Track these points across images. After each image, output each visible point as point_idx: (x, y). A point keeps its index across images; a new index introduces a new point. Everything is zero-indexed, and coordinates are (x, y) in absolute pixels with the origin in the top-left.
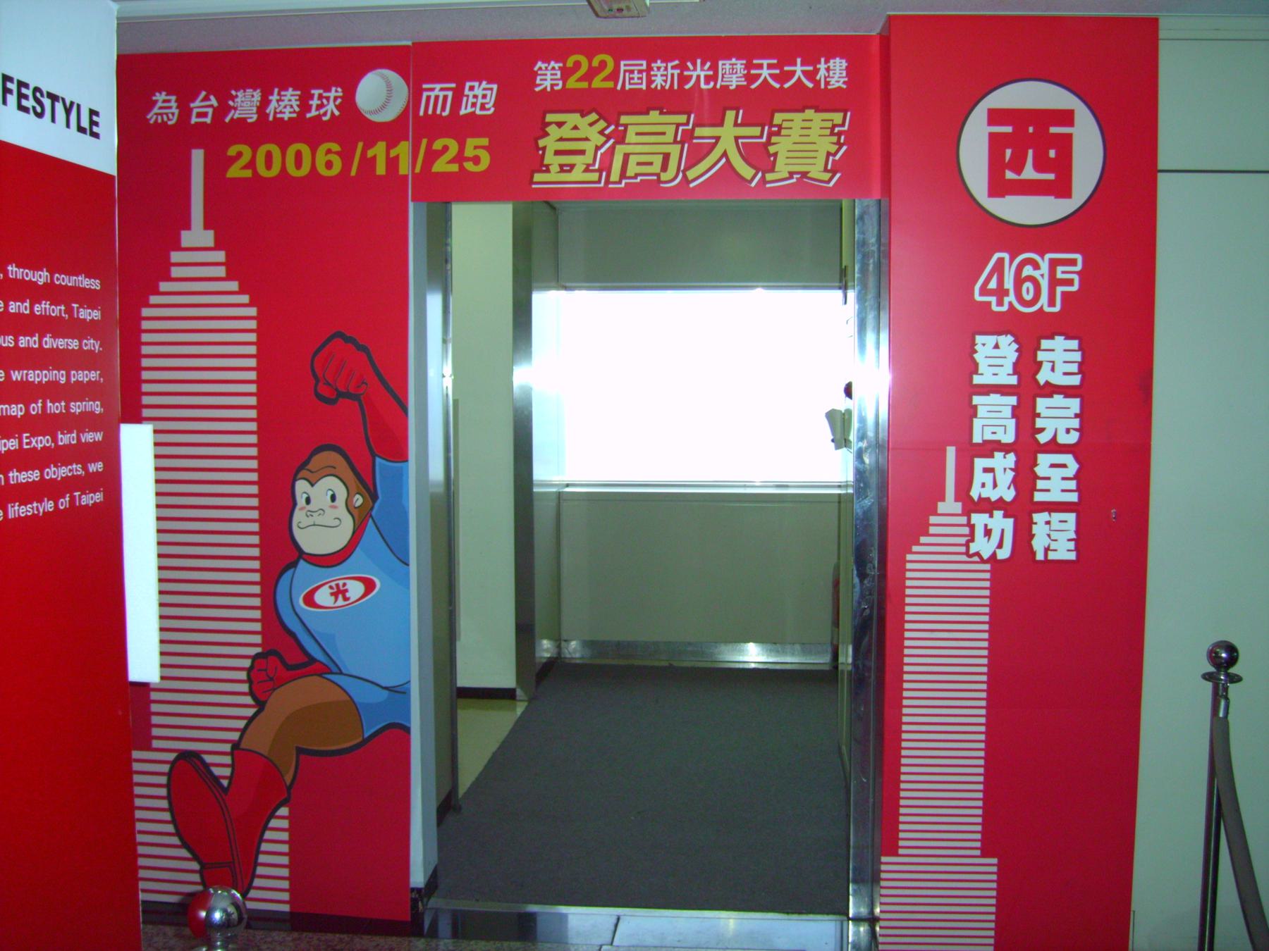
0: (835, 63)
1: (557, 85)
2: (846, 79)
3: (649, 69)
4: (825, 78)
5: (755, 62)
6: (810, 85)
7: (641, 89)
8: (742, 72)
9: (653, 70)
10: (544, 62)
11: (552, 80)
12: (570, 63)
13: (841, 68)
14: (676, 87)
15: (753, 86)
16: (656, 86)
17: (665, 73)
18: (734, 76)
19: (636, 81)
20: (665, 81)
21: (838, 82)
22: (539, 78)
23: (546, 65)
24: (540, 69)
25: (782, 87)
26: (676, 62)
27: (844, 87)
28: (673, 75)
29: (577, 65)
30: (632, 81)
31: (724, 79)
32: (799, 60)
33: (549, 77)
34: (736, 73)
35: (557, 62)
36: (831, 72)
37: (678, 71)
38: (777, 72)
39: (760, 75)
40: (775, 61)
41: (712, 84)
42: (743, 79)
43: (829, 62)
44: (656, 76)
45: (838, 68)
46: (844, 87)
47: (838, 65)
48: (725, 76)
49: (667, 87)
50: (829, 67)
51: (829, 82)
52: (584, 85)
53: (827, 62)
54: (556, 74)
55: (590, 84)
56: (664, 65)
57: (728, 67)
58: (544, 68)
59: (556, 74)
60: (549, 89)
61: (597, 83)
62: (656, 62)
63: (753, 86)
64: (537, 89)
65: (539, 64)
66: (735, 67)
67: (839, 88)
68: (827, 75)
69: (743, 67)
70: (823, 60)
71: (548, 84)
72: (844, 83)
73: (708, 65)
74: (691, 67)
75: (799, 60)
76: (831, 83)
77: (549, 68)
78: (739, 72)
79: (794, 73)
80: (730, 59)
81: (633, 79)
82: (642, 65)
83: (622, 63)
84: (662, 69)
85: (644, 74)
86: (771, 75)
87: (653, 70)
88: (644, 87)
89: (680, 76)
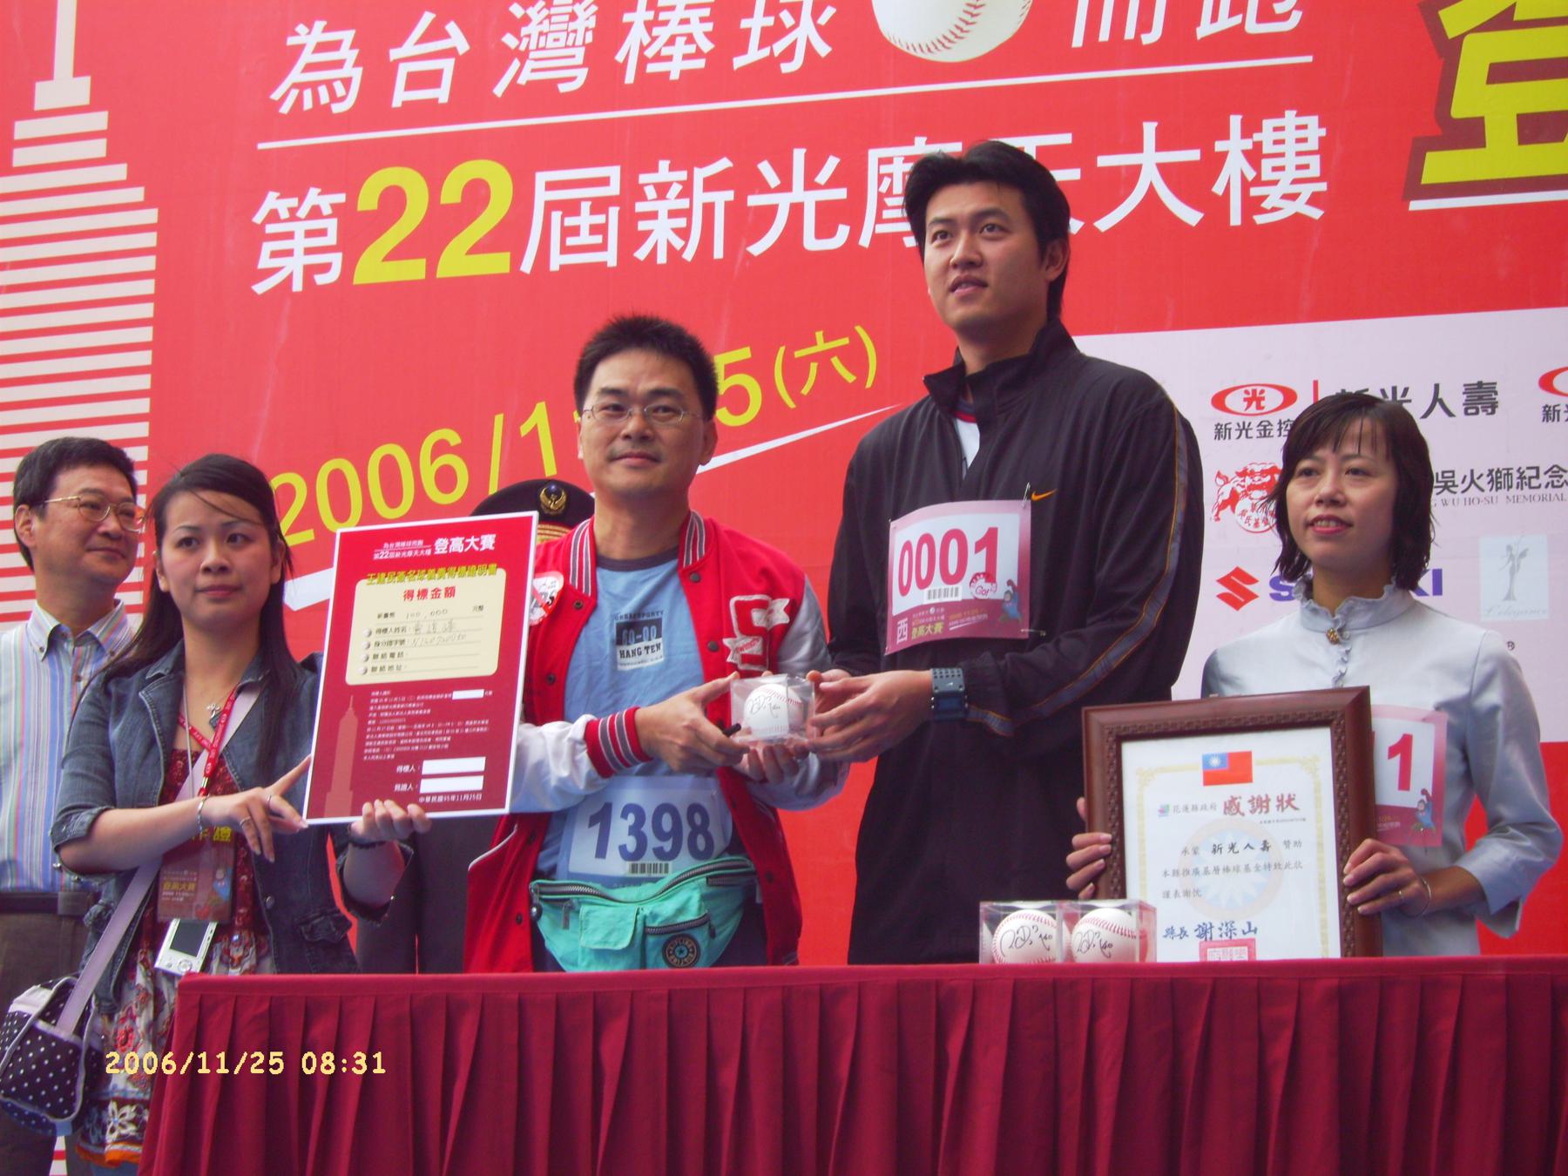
0: (1276, 129)
1: (325, 268)
2: (1322, 187)
3: (633, 191)
4: (1246, 185)
6: (1191, 217)
9: (643, 198)
11: (309, 251)
12: (368, 199)
13: (1303, 147)
14: (718, 253)
17: (683, 204)
19: (585, 238)
20: (684, 234)
21: (1293, 197)
22: (268, 247)
23: (294, 202)
26: (724, 164)
27: (1316, 213)
28: (709, 209)
29: (394, 200)
30: (571, 241)
31: (887, 214)
32: (1149, 129)
33: (299, 243)
36: (1266, 165)
37: (729, 195)
40: (1065, 139)
41: (843, 231)
43: (1259, 129)
44: (653, 215)
45: (1290, 148)
46: (1316, 213)
47: (1290, 135)
49: (689, 255)
50: (1258, 145)
51: (1263, 198)
52: (414, 270)
54: (322, 233)
55: (432, 268)
56: (683, 175)
58: (284, 214)
59: (322, 233)
60: (298, 286)
61: (457, 261)
62: (655, 169)
64: (260, 288)
65: (272, 201)
67: (1297, 217)
70: (1235, 121)
71: (294, 267)
72: (1314, 200)
73: (832, 163)
74: (773, 180)
75: (1149, 129)
76: (1266, 205)
77: (302, 213)
79: (1135, 171)
80: (911, 143)
81: (575, 231)
82: (604, 182)
83: (542, 178)
84: (676, 189)
85: (614, 212)
87: (643, 198)
88: (610, 258)
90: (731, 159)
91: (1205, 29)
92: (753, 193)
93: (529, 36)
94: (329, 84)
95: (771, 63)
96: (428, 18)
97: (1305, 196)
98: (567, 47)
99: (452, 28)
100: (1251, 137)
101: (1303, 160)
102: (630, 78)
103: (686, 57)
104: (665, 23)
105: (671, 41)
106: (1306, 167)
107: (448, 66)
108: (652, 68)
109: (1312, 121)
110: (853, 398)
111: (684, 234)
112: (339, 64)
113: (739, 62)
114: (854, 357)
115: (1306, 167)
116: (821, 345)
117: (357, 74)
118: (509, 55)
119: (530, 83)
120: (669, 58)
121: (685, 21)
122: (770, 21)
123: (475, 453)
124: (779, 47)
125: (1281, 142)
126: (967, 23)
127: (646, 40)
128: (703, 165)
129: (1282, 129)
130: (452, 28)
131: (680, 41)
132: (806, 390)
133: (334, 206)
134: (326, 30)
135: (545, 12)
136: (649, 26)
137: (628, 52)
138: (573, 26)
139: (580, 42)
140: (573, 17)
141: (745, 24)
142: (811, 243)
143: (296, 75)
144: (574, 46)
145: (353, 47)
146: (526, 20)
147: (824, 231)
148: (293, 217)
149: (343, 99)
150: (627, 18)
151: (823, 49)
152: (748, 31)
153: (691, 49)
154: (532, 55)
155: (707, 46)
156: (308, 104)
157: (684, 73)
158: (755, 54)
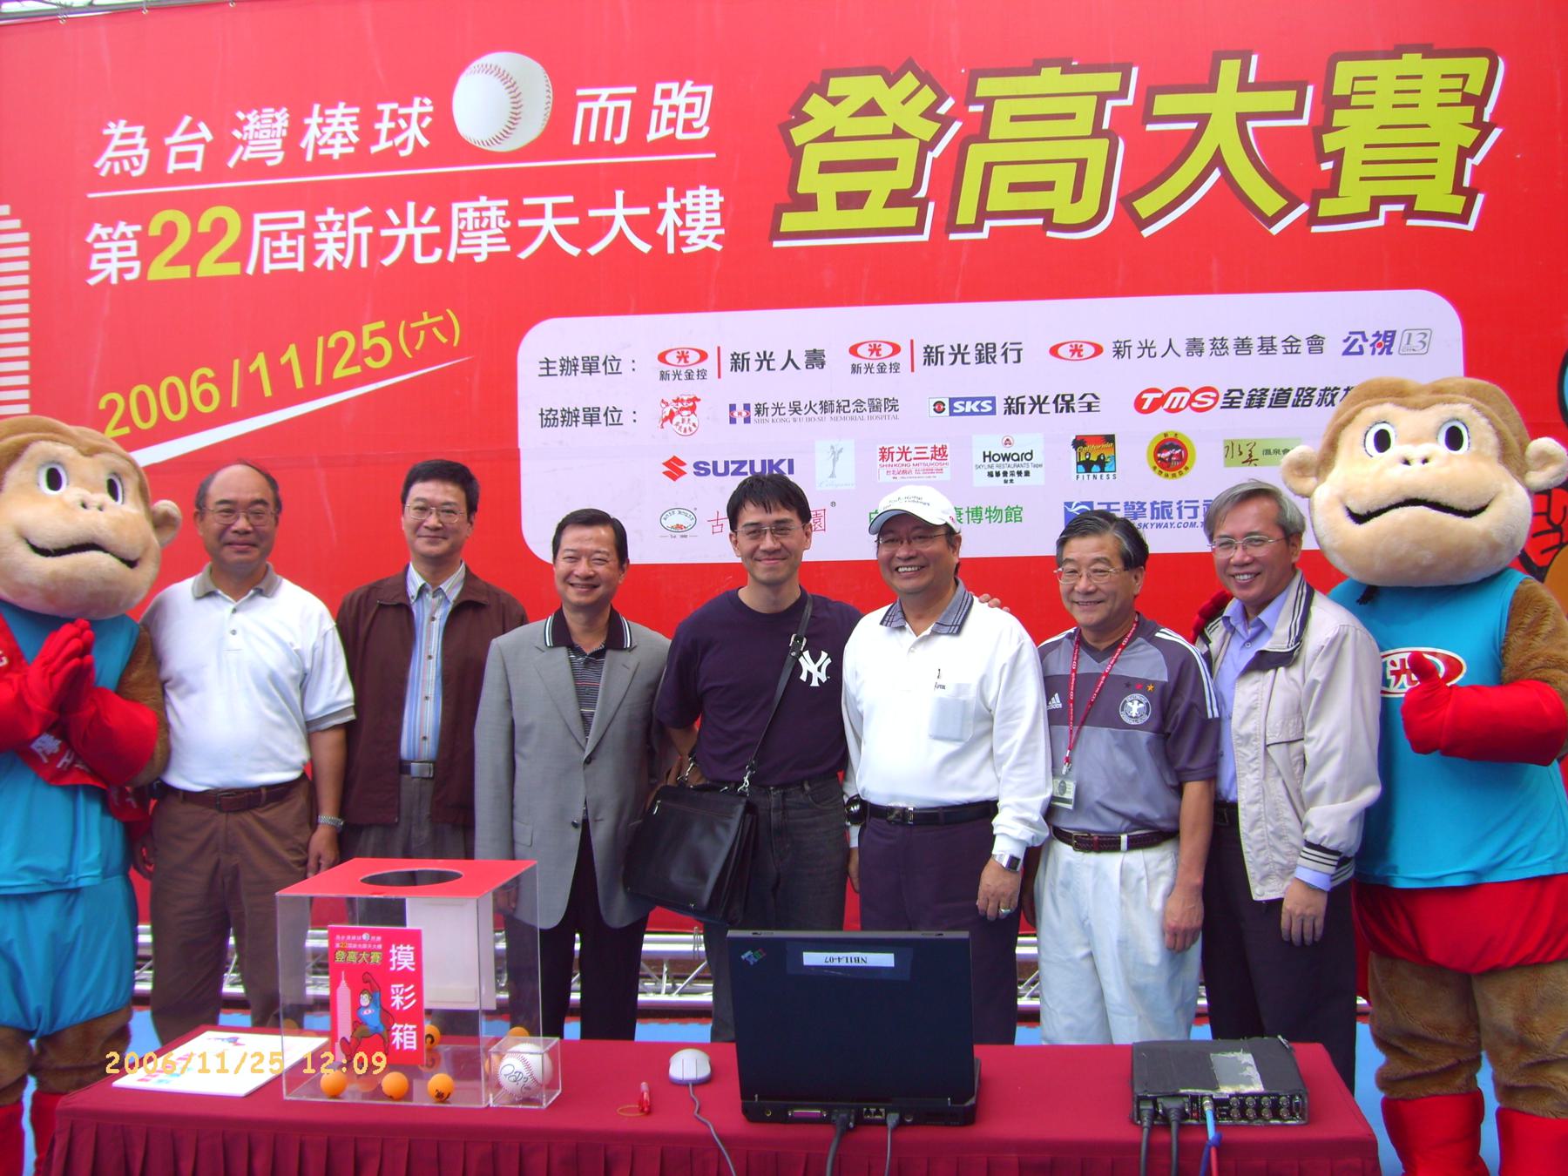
0: (694, 197)
1: (130, 270)
2: (722, 232)
3: (312, 226)
4: (677, 229)
5: (528, 201)
6: (645, 248)
7: (295, 271)
8: (502, 225)
9: (319, 230)
10: (105, 225)
11: (121, 260)
12: (155, 229)
14: (364, 263)
15: (524, 255)
16: (325, 264)
17: (343, 234)
18: (484, 234)
19: (285, 254)
20: (343, 252)
21: (704, 237)
22: (96, 257)
23: (110, 230)
24: (99, 239)
25: (584, 254)
26: (366, 211)
27: (718, 247)
28: (358, 238)
29: (170, 230)
30: (276, 256)
31: (464, 242)
32: (620, 195)
33: (115, 255)
34: (488, 227)
35: (130, 223)
36: (689, 218)
37: (370, 229)
38: (575, 221)
39: (538, 229)
40: (569, 199)
41: (438, 252)
42: (503, 240)
43: (684, 196)
44: (324, 241)
45: (703, 208)
46: (718, 247)
47: (703, 200)
48: (465, 235)
49: (346, 265)
50: (684, 206)
51: (687, 237)
52: (183, 272)
53: (679, 196)
54: (128, 249)
55: (194, 271)
56: (342, 217)
57: (470, 215)
58: (105, 237)
59: (128, 249)
60: (114, 281)
61: (209, 267)
62: (324, 213)
63: (524, 255)
64: (92, 281)
65: (98, 229)
66: (485, 214)
67: (707, 250)
68: (679, 223)
69: (503, 213)
70: (670, 192)
71: (112, 269)
72: (717, 239)
73: (431, 211)
74: (396, 220)
75: (620, 195)
78: (493, 225)
79: (611, 219)
81: (278, 250)
82: (295, 220)
83: (258, 217)
84: (338, 225)
85: (301, 239)
86: (558, 228)
87: (319, 230)
88: (300, 266)
89: (373, 238)
90: (370, 208)
91: (652, 136)
92: (384, 228)
93: (248, 131)
94: (129, 158)
95: (393, 151)
96: (187, 120)
97: (712, 237)
98: (271, 138)
99: (202, 126)
100: (680, 201)
101: (710, 216)
102: (309, 157)
103: (343, 146)
104: (330, 125)
105: (334, 136)
106: (712, 219)
107: (200, 149)
108: (323, 152)
109: (716, 192)
110: (446, 352)
111: (343, 252)
112: (134, 147)
113: (374, 149)
114: (446, 327)
115: (712, 219)
116: (427, 321)
117: (146, 153)
118: (236, 143)
119: (251, 161)
120: (332, 146)
121: (342, 124)
122: (392, 125)
123: (223, 382)
124: (398, 140)
125: (694, 204)
126: (510, 128)
127: (319, 134)
128: (354, 210)
129: (697, 196)
130: (202, 126)
131: (339, 136)
132: (418, 347)
133: (135, 233)
134: (127, 126)
135: (258, 117)
136: (320, 126)
137: (308, 142)
138: (274, 126)
139: (278, 136)
140: (275, 120)
141: (378, 126)
142: (419, 259)
143: (110, 153)
144: (275, 138)
145: (144, 135)
146: (246, 122)
147: (427, 251)
148: (111, 239)
149: (137, 168)
150: (307, 121)
151: (425, 142)
152: (379, 131)
153: (346, 141)
154: (252, 143)
155: (355, 139)
156: (117, 171)
157: (342, 156)
158: (383, 145)
